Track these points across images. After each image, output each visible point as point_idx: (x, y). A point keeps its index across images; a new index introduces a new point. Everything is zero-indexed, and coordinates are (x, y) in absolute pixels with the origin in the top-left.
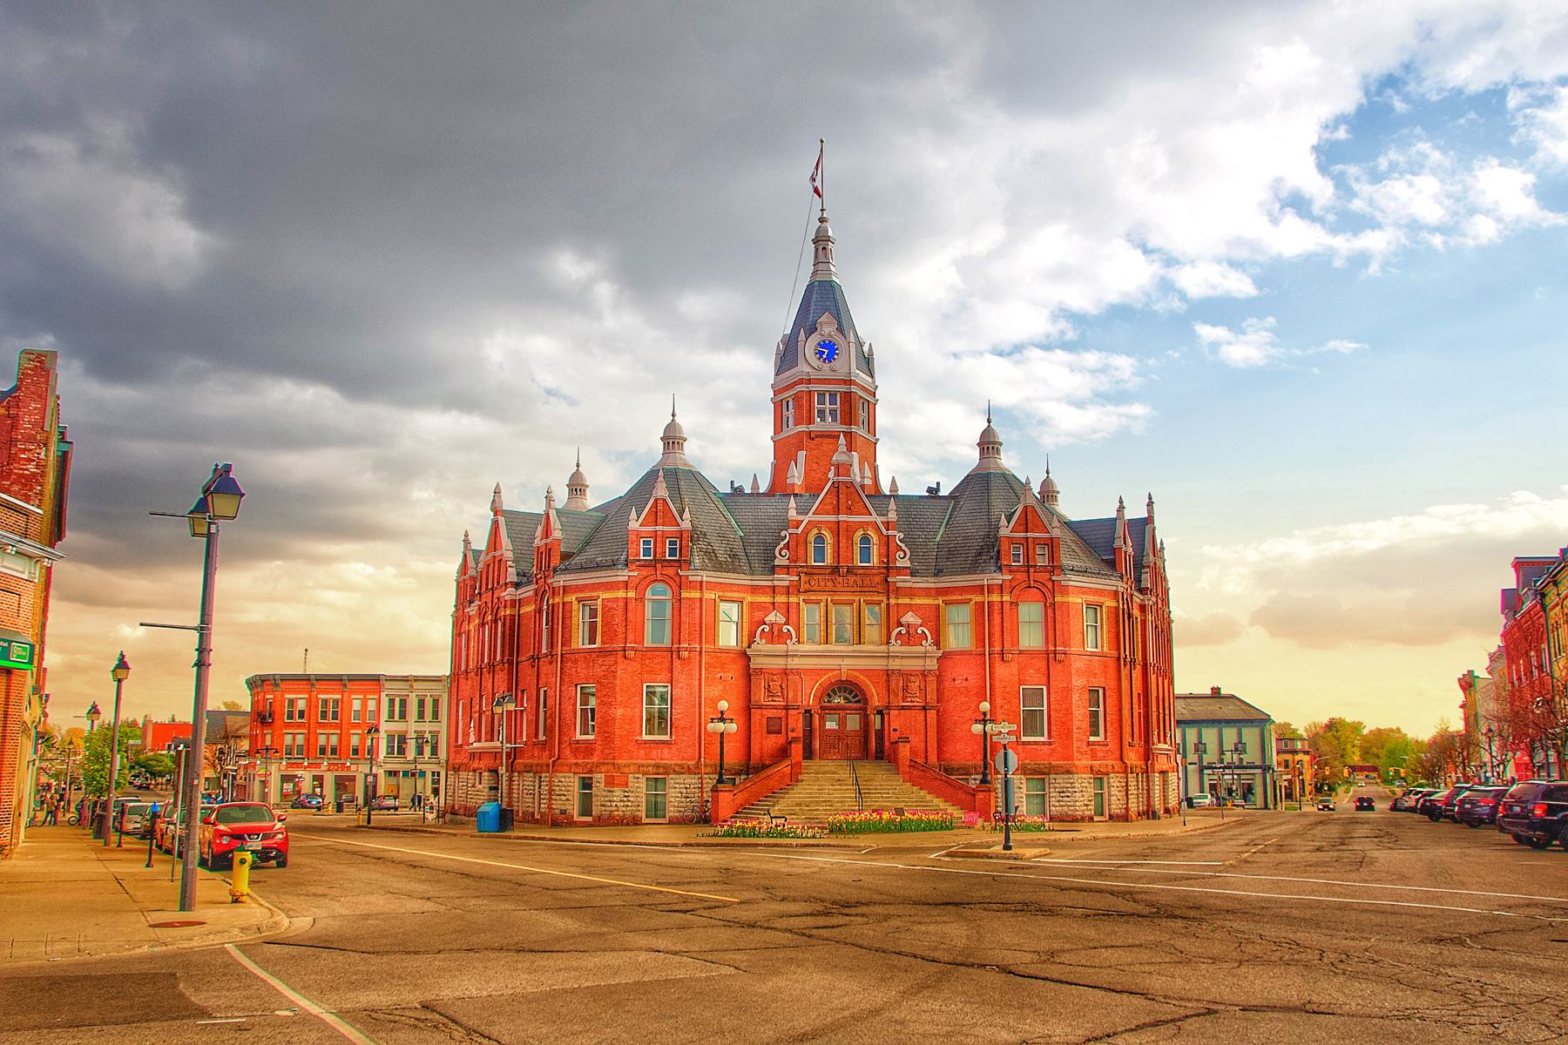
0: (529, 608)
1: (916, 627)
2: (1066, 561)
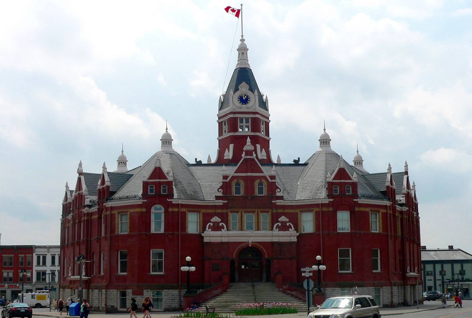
0: (96, 217)
1: (286, 222)
2: (360, 191)
